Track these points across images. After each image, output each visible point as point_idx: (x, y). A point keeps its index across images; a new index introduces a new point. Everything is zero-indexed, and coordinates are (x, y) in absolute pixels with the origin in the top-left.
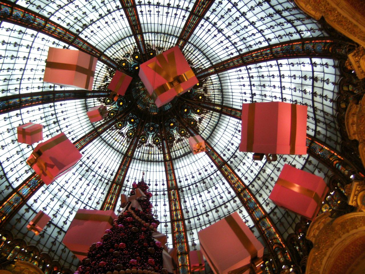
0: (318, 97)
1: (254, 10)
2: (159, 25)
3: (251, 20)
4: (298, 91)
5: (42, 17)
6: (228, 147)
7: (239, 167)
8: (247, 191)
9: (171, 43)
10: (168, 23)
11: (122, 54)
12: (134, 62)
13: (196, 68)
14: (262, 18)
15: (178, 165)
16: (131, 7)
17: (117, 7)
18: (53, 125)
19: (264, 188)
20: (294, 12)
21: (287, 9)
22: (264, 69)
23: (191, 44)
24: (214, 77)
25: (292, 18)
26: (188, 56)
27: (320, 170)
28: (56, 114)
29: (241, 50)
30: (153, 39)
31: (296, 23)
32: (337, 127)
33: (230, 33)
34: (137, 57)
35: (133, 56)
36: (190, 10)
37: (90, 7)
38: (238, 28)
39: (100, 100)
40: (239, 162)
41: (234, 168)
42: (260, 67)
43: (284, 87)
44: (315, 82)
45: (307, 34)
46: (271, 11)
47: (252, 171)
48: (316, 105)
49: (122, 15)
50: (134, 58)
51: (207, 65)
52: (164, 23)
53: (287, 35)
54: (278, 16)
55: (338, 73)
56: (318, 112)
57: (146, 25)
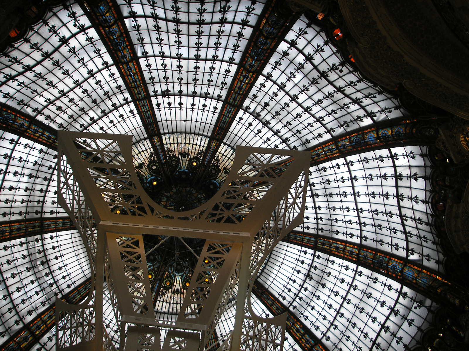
0: (406, 200)
1: (308, 90)
2: (183, 122)
3: (305, 105)
4: (377, 197)
5: (27, 116)
6: (289, 287)
8: (321, 347)
10: (194, 119)
12: (151, 174)
14: (319, 100)
16: (143, 99)
17: (125, 99)
18: (41, 268)
19: (344, 340)
20: (361, 85)
21: (351, 84)
22: (329, 171)
23: (227, 144)
25: (359, 95)
26: (224, 163)
27: (421, 304)
30: (176, 142)
31: (366, 102)
32: (437, 239)
33: (279, 126)
34: (154, 167)
35: (149, 167)
36: (223, 98)
38: (289, 118)
40: (305, 306)
42: (324, 169)
43: (358, 193)
44: (399, 180)
45: (381, 117)
46: (330, 89)
47: (325, 318)
48: (404, 211)
49: (131, 111)
52: (189, 118)
53: (355, 120)
54: (340, 95)
55: (429, 163)
56: (409, 222)
57: (164, 123)
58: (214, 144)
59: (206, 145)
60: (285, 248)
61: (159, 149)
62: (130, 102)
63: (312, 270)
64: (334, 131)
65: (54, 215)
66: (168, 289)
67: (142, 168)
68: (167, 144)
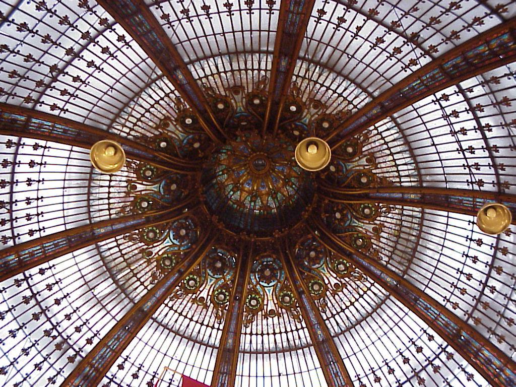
7: (500, 331)
9: (259, 70)
11: (151, 124)
13: (337, 114)
15: (345, 347)
17: (103, 22)
24: (384, 125)
28: (34, 295)
29: (433, 48)
34: (189, 121)
35: (180, 121)
37: (36, 41)
39: (131, 239)
40: (497, 319)
41: (487, 335)
42: (496, 80)
50: (183, 124)
51: (362, 100)
58: (284, 63)
59: (269, 67)
60: (444, 220)
61: (189, 89)
62: (114, 24)
63: (499, 255)
64: (505, 11)
65: (36, 235)
66: (254, 313)
67: (168, 125)
68: (200, 79)
